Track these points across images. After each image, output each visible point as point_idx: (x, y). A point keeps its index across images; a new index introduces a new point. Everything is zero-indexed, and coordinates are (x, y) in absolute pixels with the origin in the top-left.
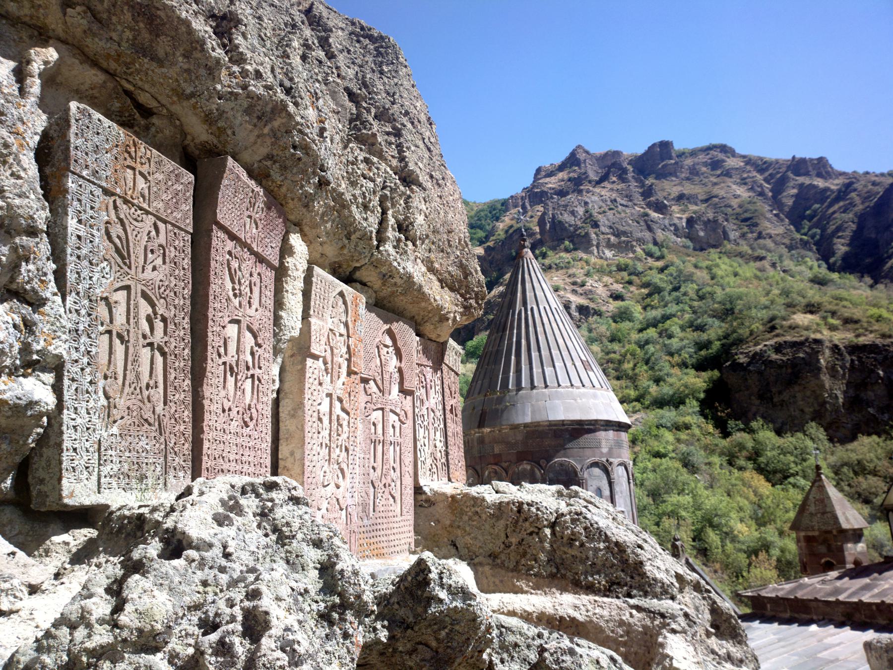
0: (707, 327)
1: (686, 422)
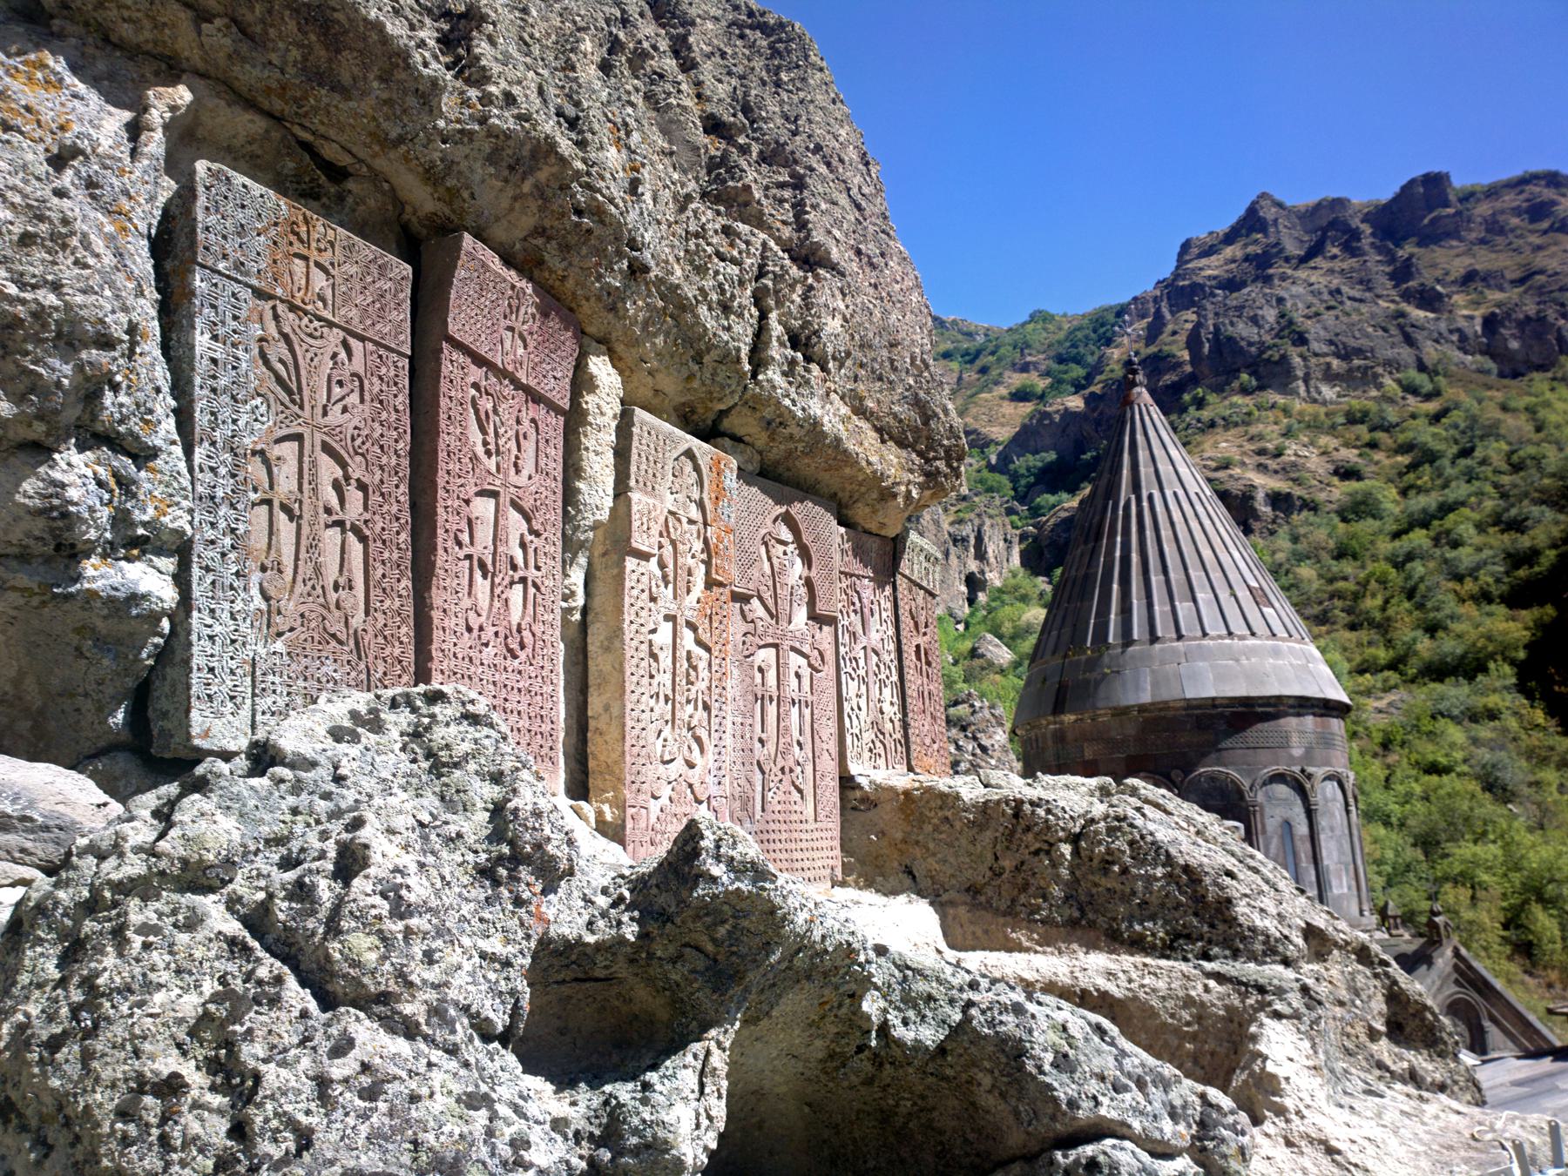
0: (1529, 523)
1: (1490, 705)
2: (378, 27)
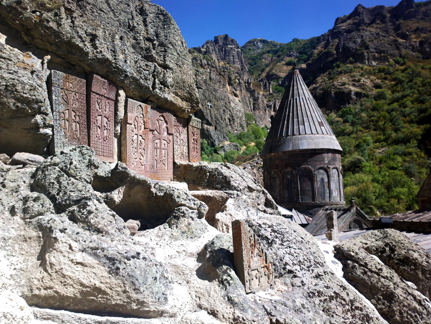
0: (426, 101)
2: (78, 45)
